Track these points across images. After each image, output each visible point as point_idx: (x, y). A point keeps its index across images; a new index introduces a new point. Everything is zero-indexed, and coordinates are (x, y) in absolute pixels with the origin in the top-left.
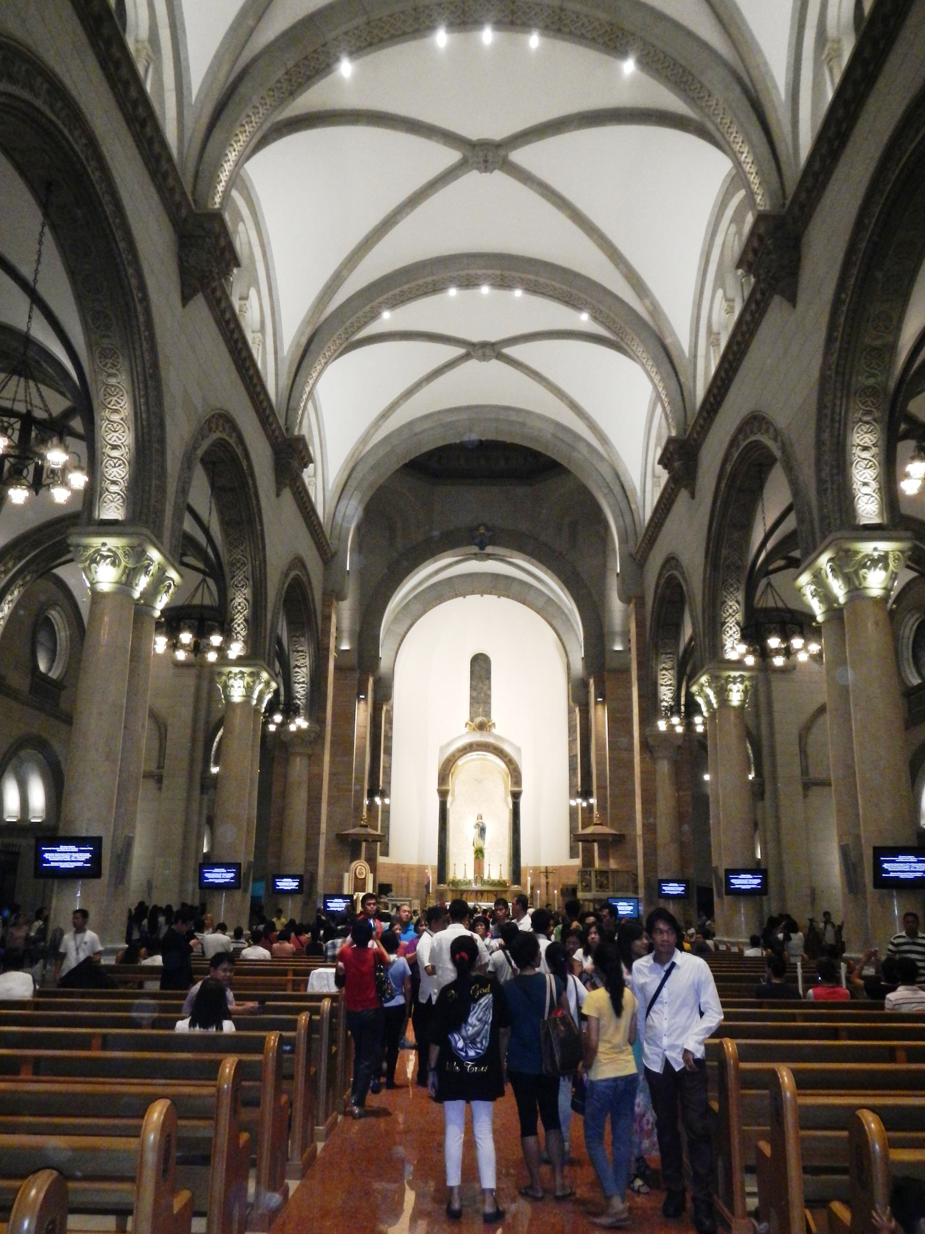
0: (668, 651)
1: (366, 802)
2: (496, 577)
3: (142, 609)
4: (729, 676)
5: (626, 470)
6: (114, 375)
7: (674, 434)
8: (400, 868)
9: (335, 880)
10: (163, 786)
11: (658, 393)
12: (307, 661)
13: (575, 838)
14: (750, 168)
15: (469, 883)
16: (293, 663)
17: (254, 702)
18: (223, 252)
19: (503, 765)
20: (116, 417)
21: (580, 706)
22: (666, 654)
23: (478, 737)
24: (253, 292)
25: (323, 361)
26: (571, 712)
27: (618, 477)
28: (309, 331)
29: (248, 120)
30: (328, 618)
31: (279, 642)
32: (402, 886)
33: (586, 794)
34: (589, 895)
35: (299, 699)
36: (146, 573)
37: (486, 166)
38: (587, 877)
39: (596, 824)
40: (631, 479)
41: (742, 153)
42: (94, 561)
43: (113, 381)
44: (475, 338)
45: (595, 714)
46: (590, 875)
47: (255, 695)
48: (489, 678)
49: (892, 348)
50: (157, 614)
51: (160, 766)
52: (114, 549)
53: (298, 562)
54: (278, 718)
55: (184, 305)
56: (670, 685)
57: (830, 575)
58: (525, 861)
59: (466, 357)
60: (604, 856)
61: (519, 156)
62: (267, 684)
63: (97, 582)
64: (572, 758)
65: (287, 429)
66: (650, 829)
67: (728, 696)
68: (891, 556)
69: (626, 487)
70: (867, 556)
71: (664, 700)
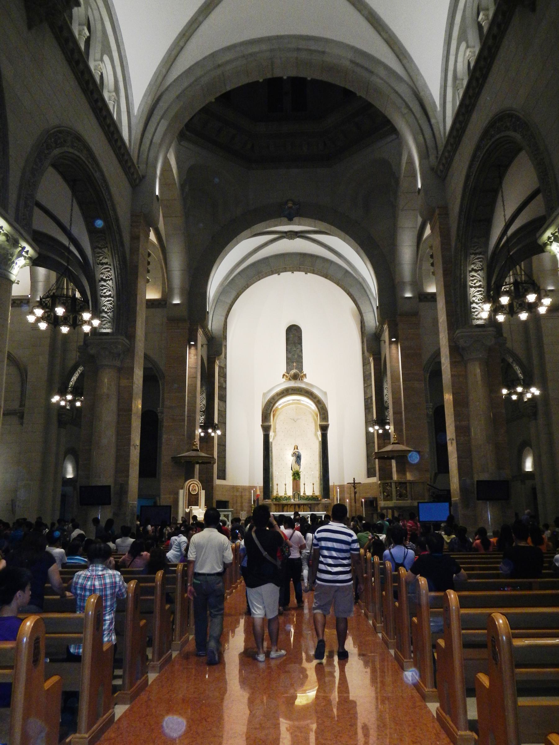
0: (477, 251)
1: (199, 432)
2: (304, 256)
5: (425, 85)
8: (235, 488)
9: (172, 496)
10: (24, 421)
12: (112, 274)
15: (289, 498)
22: (475, 254)
23: (293, 384)
26: (365, 363)
30: (135, 238)
32: (237, 502)
33: (381, 421)
34: (390, 504)
35: (106, 313)
38: (388, 488)
39: (393, 443)
40: (431, 94)
45: (390, 352)
46: (391, 486)
48: (301, 343)
51: (22, 405)
56: (480, 286)
58: (333, 480)
71: (474, 302)
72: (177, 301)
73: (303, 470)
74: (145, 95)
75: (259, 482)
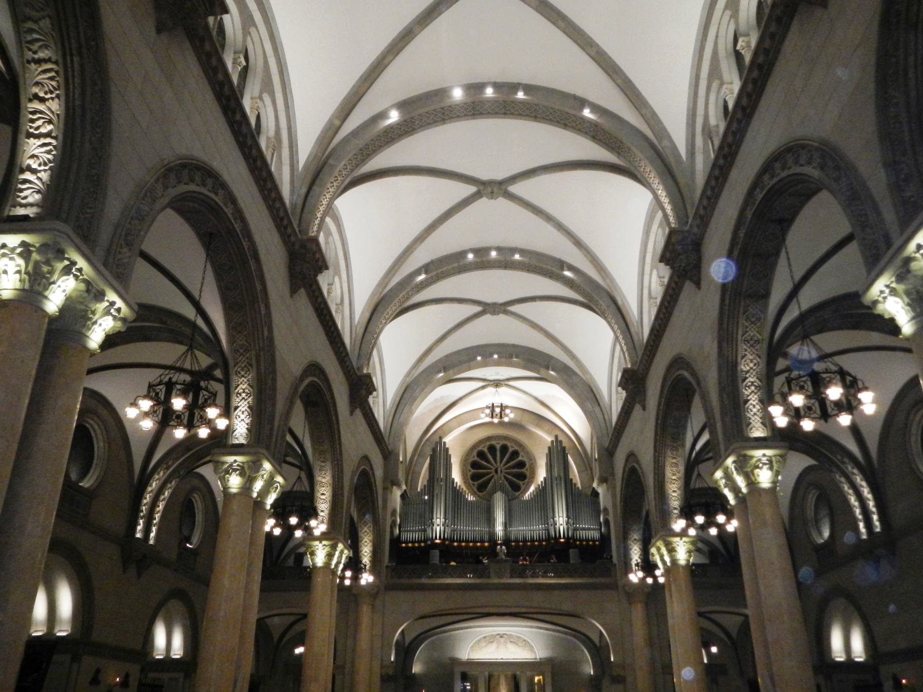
3: (258, 504)
7: (629, 366)
11: (617, 338)
14: (665, 200)
17: (333, 567)
24: (337, 279)
28: (375, 300)
29: (336, 179)
30: (385, 501)
31: (352, 519)
37: (492, 195)
41: (659, 190)
44: (489, 300)
50: (268, 507)
52: (241, 464)
55: (291, 296)
57: (735, 473)
61: (514, 189)
62: (342, 552)
63: (229, 488)
70: (759, 460)
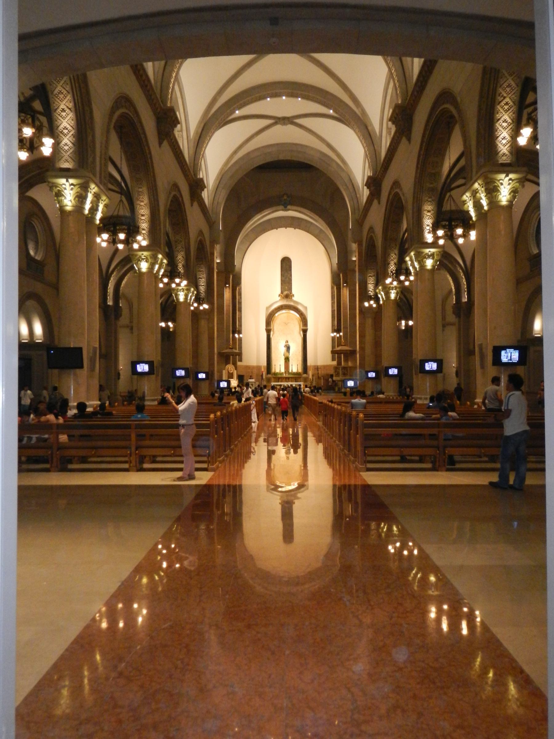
2: (293, 218)
4: (390, 287)
5: (355, 177)
6: (141, 188)
8: (247, 367)
12: (205, 276)
13: (333, 352)
15: (282, 373)
16: (198, 277)
17: (189, 301)
18: (174, 121)
19: (298, 316)
20: (142, 204)
21: (336, 286)
22: (371, 269)
25: (208, 138)
26: (332, 288)
27: (351, 180)
28: (202, 125)
33: (338, 331)
36: (158, 264)
40: (357, 182)
42: (139, 260)
43: (140, 190)
44: (280, 115)
47: (189, 298)
48: (291, 270)
49: (439, 174)
51: (131, 322)
53: (201, 233)
54: (196, 305)
55: (160, 146)
56: (373, 284)
58: (310, 362)
59: (275, 124)
60: (346, 360)
63: (141, 268)
64: (333, 311)
65: (194, 175)
66: (362, 348)
67: (390, 295)
68: (435, 254)
69: (355, 186)
70: (427, 254)
71: (370, 291)
72: (218, 261)
73: (291, 355)
74: (215, 180)
75: (264, 363)
